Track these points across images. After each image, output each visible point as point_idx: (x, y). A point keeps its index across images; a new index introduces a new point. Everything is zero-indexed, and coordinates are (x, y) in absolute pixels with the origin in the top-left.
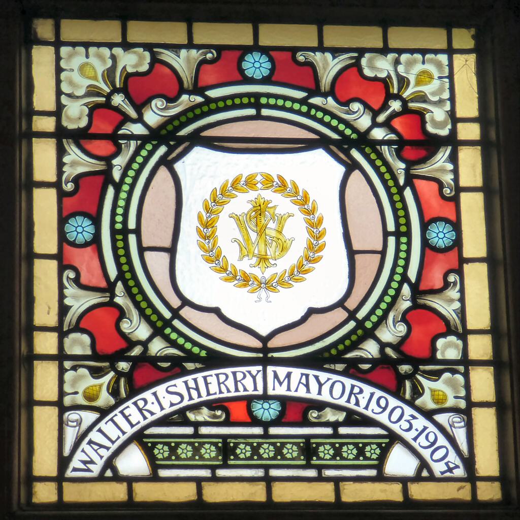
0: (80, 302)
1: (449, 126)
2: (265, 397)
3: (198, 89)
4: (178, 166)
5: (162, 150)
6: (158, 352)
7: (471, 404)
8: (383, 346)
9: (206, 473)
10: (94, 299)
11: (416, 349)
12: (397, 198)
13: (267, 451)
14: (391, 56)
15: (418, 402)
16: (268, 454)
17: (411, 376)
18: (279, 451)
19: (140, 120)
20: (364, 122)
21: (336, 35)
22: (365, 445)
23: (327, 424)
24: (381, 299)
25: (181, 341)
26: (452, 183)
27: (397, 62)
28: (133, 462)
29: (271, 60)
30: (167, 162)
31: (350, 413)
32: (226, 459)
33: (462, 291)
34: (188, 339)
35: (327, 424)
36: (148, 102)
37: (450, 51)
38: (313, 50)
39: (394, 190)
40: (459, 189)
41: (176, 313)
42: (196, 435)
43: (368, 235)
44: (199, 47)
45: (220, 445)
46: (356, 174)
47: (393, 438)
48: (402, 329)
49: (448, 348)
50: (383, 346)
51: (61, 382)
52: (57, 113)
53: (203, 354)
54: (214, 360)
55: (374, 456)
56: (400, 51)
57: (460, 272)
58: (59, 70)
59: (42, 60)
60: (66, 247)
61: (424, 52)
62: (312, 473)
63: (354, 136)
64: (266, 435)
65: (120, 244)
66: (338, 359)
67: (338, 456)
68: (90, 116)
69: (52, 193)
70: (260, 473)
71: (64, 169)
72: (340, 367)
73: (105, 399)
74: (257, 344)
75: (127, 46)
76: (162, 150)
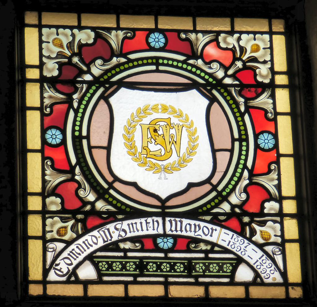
1: (270, 77)
2: (165, 235)
4: (112, 100)
5: (101, 90)
6: (101, 208)
8: (233, 206)
9: (131, 279)
11: (252, 208)
13: (165, 267)
15: (254, 239)
16: (166, 269)
17: (249, 224)
18: (172, 267)
19: (89, 72)
21: (203, 24)
23: (201, 251)
24: (231, 179)
26: (273, 111)
27: (239, 39)
28: (87, 272)
29: (165, 37)
30: (105, 98)
31: (214, 245)
33: (279, 175)
35: (201, 251)
36: (93, 61)
37: (271, 33)
38: (191, 32)
39: (238, 114)
43: (223, 140)
44: (122, 29)
46: (216, 105)
47: (239, 260)
49: (271, 207)
50: (233, 206)
51: (44, 225)
53: (128, 210)
55: (229, 271)
56: (241, 33)
57: (278, 163)
58: (41, 42)
59: (31, 37)
60: (46, 146)
61: (255, 33)
62: (192, 280)
63: (214, 82)
64: (166, 258)
66: (207, 213)
68: (60, 69)
69: (37, 114)
70: (162, 279)
72: (208, 218)
73: (70, 235)
74: (158, 203)
75: (80, 28)
76: (101, 90)
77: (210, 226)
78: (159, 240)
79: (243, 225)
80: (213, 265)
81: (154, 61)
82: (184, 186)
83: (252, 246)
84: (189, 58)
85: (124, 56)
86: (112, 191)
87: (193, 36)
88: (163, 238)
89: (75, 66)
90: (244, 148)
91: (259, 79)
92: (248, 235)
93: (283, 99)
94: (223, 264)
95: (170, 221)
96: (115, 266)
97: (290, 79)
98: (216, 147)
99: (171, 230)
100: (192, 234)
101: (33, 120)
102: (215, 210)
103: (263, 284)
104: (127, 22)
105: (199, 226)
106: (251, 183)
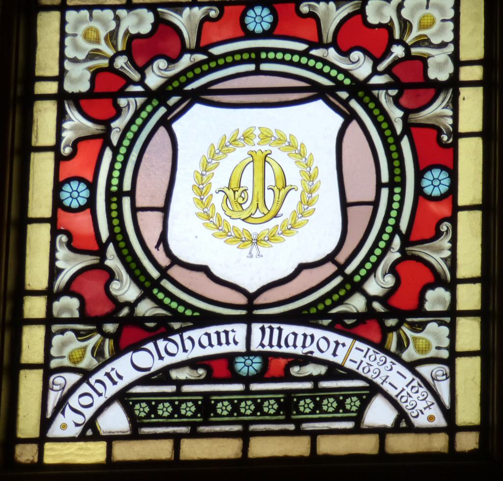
2: (249, 353)
5: (162, 111)
6: (146, 311)
7: (454, 354)
8: (370, 299)
10: (88, 260)
12: (393, 148)
13: (246, 408)
22: (263, 400)
24: (371, 252)
28: (115, 420)
30: (166, 123)
32: (206, 416)
34: (173, 298)
36: (150, 63)
41: (164, 272)
43: (362, 188)
45: (200, 403)
46: (354, 125)
47: (374, 389)
48: (390, 281)
49: (436, 299)
53: (189, 313)
55: (354, 409)
57: (453, 220)
58: (63, 34)
59: (48, 25)
60: (60, 212)
62: (292, 427)
64: (247, 391)
65: (114, 206)
66: (324, 314)
68: (92, 80)
71: (64, 134)
72: (326, 322)
74: (242, 300)
76: (162, 111)
81: (253, 56)
82: (290, 270)
83: (398, 367)
86: (165, 283)
90: (397, 198)
92: (393, 348)
93: (472, 110)
94: (263, 400)
97: (486, 73)
99: (262, 345)
101: (42, 168)
103: (411, 429)
105: (312, 337)
106: (405, 256)
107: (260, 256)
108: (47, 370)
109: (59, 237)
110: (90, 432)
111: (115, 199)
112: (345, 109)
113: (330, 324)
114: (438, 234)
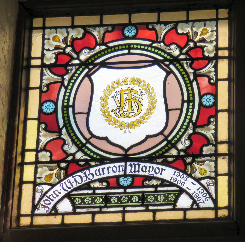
0: (45, 138)
3: (103, 43)
4: (93, 77)
5: (87, 70)
7: (217, 174)
8: (179, 151)
12: (189, 85)
13: (125, 199)
14: (191, 24)
16: (125, 200)
17: (190, 164)
18: (130, 199)
19: (78, 58)
20: (176, 52)
21: (165, 16)
24: (179, 130)
25: (89, 152)
28: (65, 206)
30: (88, 76)
31: (163, 180)
34: (92, 151)
37: (217, 20)
39: (188, 82)
40: (218, 80)
42: (94, 194)
43: (175, 101)
46: (171, 76)
47: (181, 191)
52: (42, 58)
54: (103, 161)
55: (172, 200)
57: (216, 117)
58: (44, 39)
64: (125, 192)
67: (119, 202)
68: (56, 58)
69: (38, 91)
70: (121, 209)
71: (43, 82)
72: (159, 160)
73: (54, 180)
74: (122, 152)
75: (73, 27)
76: (87, 70)
77: (161, 167)
78: (121, 180)
79: (186, 164)
80: (160, 196)
84: (153, 42)
85: (105, 44)
86: (88, 145)
87: (157, 27)
88: (124, 178)
89: (69, 55)
90: (191, 107)
91: (206, 54)
92: (189, 173)
95: (131, 165)
96: (89, 200)
98: (169, 108)
100: (147, 174)
102: (166, 155)
103: (199, 208)
104: (109, 19)
105: (153, 167)
106: (195, 133)
107: (129, 132)
108: (35, 183)
109: (41, 125)
110: (54, 212)
111: (65, 109)
112: (168, 69)
113: (162, 162)
114: (209, 123)
